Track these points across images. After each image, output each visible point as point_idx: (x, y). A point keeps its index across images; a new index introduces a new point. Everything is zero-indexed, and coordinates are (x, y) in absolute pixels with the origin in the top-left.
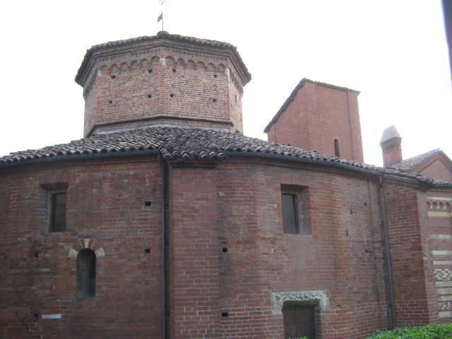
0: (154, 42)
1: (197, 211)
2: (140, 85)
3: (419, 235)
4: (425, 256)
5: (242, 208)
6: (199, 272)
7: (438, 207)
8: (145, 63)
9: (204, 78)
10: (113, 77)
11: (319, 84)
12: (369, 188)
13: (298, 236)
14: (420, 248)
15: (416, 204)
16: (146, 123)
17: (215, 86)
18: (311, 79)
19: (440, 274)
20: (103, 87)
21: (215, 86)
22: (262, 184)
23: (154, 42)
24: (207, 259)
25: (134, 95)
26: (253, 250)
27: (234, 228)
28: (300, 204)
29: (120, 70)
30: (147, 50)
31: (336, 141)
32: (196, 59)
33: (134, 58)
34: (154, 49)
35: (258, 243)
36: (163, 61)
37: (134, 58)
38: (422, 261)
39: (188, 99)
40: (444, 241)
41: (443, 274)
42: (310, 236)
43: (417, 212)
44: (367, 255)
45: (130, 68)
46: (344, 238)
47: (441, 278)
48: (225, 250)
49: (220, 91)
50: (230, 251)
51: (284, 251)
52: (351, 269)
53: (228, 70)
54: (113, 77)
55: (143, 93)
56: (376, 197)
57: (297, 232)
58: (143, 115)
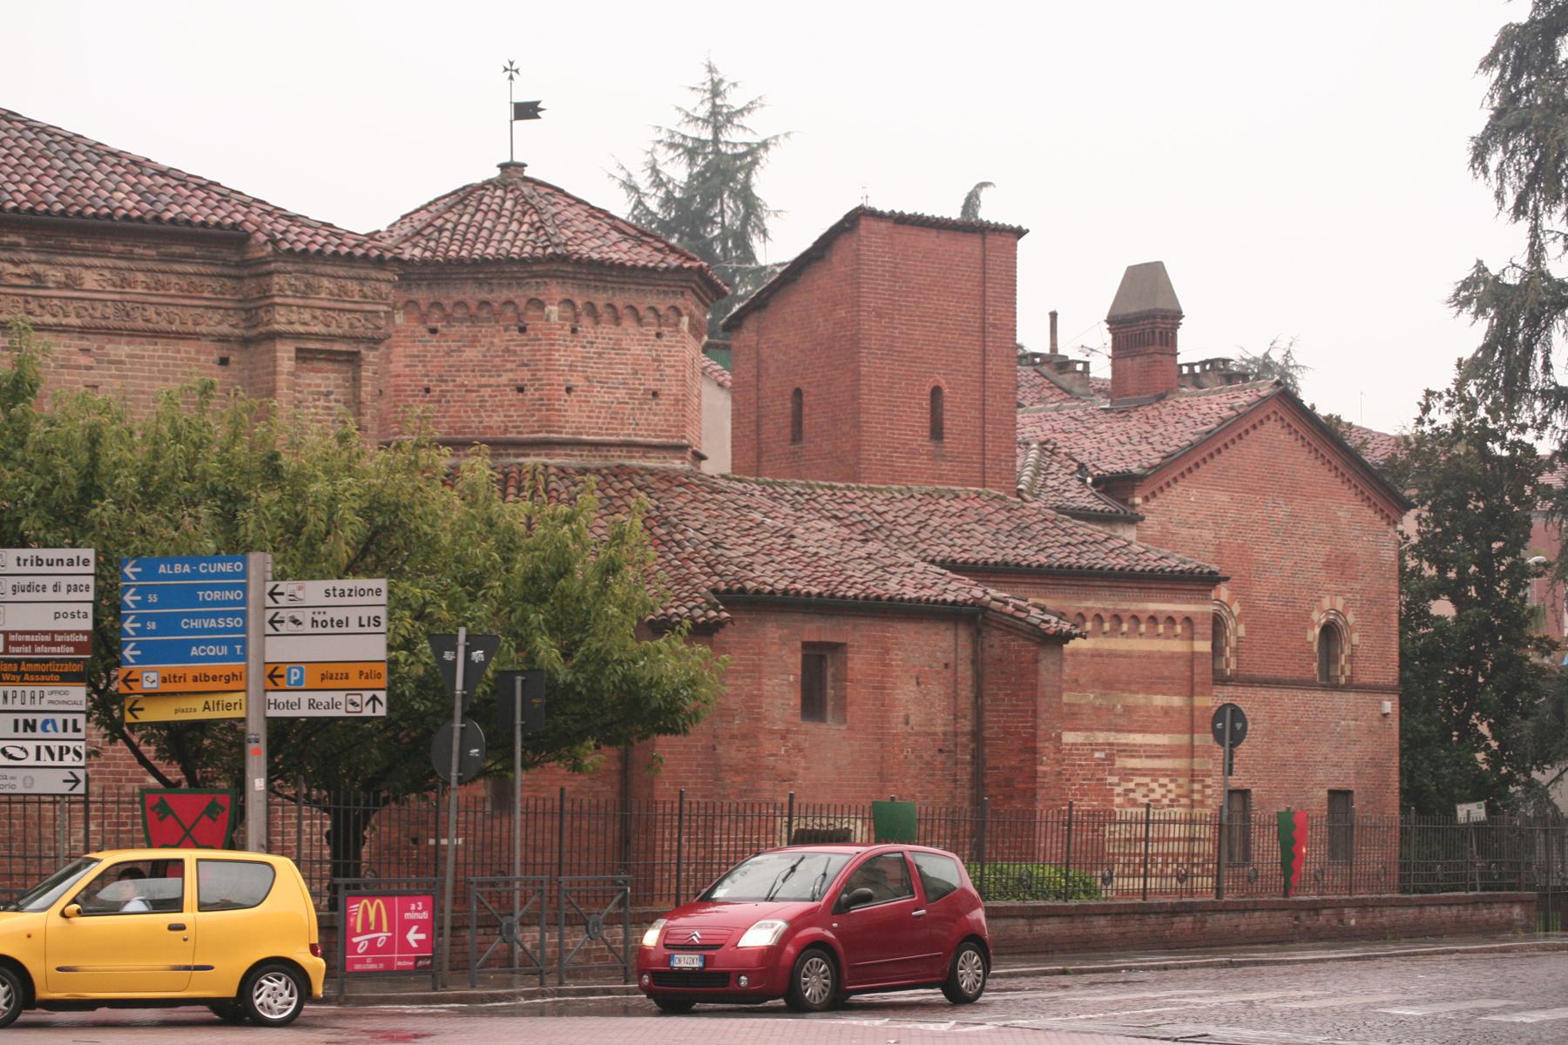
2: (498, 361)
3: (1034, 727)
5: (740, 682)
7: (1161, 628)
8: (509, 312)
9: (635, 342)
10: (434, 331)
11: (900, 220)
13: (824, 726)
14: (1034, 750)
15: (1036, 672)
18: (879, 209)
19: (1143, 790)
25: (484, 381)
28: (830, 672)
29: (448, 319)
30: (519, 281)
31: (936, 392)
33: (484, 295)
35: (761, 738)
36: (553, 310)
37: (484, 295)
38: (1036, 772)
39: (600, 396)
40: (1166, 711)
41: (1153, 791)
42: (843, 727)
43: (1034, 687)
45: (473, 319)
49: (669, 371)
50: (720, 750)
51: (801, 750)
53: (686, 319)
54: (434, 331)
55: (504, 379)
57: (823, 720)
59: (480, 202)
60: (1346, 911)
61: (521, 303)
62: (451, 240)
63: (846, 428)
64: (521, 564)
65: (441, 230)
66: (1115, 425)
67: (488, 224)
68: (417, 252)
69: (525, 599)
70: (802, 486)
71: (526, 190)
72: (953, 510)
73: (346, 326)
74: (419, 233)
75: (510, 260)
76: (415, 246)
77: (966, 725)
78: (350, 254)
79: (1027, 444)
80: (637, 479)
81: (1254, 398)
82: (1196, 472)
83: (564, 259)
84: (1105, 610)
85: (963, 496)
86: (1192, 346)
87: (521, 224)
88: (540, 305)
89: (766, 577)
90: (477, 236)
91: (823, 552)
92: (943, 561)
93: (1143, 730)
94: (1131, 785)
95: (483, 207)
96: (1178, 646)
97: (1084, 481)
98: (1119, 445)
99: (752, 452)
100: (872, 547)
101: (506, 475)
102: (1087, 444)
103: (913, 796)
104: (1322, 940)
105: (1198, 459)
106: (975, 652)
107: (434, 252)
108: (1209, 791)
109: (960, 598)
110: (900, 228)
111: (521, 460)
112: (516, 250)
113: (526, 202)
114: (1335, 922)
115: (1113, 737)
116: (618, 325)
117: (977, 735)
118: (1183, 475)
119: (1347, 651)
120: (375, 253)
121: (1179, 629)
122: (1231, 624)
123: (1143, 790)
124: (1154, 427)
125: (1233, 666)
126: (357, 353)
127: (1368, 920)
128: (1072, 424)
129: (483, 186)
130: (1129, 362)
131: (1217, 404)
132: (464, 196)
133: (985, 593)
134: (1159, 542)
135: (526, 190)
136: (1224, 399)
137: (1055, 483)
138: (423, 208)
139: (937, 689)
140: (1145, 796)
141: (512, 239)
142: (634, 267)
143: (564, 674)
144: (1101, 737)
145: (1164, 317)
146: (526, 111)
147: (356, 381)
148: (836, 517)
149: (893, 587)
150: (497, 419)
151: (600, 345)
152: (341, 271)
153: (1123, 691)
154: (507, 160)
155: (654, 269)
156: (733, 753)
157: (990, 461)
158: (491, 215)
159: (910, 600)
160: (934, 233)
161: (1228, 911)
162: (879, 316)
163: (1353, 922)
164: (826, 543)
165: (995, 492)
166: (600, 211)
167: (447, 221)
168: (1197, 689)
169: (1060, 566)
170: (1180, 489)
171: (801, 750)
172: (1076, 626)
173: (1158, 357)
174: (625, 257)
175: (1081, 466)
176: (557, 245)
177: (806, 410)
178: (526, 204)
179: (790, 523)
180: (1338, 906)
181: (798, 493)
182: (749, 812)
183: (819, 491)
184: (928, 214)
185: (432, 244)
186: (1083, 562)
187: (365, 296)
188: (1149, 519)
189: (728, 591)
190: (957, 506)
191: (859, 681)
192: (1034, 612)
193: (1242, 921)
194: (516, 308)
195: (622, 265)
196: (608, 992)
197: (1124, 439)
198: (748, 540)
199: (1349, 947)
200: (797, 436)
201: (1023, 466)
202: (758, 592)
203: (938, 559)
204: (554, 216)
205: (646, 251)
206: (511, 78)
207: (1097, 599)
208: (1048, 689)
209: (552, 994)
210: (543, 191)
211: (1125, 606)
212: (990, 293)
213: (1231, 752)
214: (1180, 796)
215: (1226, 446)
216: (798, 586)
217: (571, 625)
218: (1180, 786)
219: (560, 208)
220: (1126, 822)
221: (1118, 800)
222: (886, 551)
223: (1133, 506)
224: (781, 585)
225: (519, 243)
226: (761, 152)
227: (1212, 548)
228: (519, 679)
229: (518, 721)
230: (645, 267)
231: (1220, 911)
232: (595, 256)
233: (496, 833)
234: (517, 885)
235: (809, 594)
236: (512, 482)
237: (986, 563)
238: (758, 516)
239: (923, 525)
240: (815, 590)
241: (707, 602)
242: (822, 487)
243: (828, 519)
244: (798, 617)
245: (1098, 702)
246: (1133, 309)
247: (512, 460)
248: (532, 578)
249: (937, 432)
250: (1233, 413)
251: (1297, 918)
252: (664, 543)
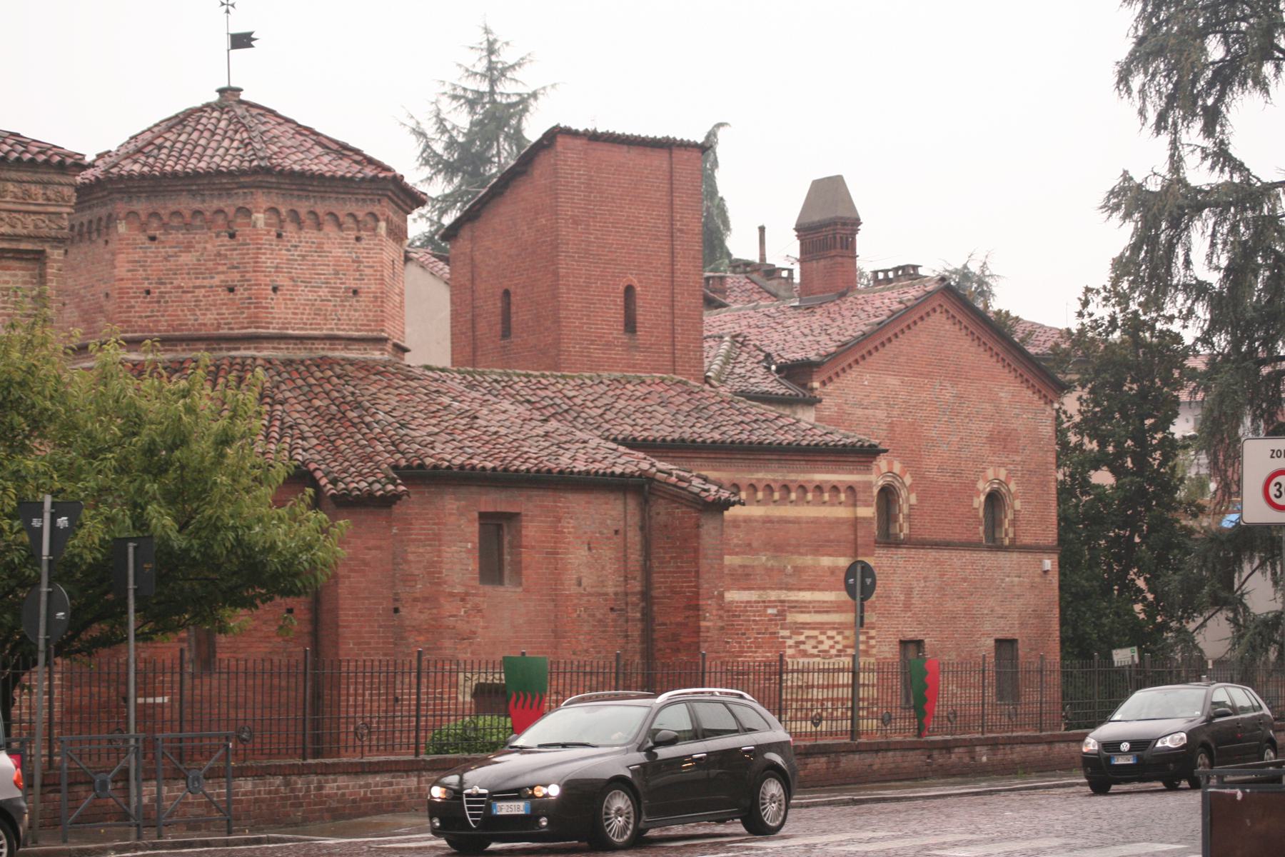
0: (242, 180)
1: (367, 564)
2: (210, 264)
4: (705, 619)
6: (369, 643)
7: (826, 496)
8: (220, 220)
9: (336, 246)
10: (153, 239)
11: (594, 137)
12: (625, 504)
13: (501, 589)
14: (697, 608)
15: (698, 536)
16: (224, 346)
17: (357, 261)
18: (574, 128)
19: (813, 642)
20: (131, 257)
21: (357, 261)
22: (451, 514)
23: (242, 180)
24: (380, 626)
25: (198, 282)
26: (435, 611)
27: (409, 579)
28: (507, 539)
30: (226, 192)
31: (629, 290)
32: (321, 209)
33: (197, 205)
34: (241, 191)
35: (442, 600)
36: (260, 218)
38: (699, 627)
39: (304, 294)
40: (833, 571)
41: (821, 642)
42: (520, 589)
43: (696, 550)
44: (612, 615)
45: (188, 227)
46: (574, 589)
47: (815, 651)
48: (396, 610)
49: (368, 271)
50: (403, 612)
51: (479, 611)
52: (581, 637)
53: (383, 225)
54: (153, 239)
55: (217, 280)
56: (637, 519)
57: (501, 583)
58: (219, 327)
59: (198, 122)
60: (978, 749)
61: (230, 211)
62: (169, 156)
63: (548, 323)
64: (140, 441)
65: (160, 147)
66: (801, 320)
67: (203, 142)
68: (137, 167)
69: (146, 470)
70: (500, 375)
71: (240, 111)
72: (638, 394)
73: (31, 227)
74: (139, 151)
75: (219, 173)
76: (135, 162)
77: (636, 586)
78: (32, 161)
79: (721, 337)
80: (338, 370)
81: (921, 293)
82: (869, 359)
83: (268, 171)
84: (774, 481)
85: (649, 382)
86: (874, 252)
87: (232, 140)
88: (248, 213)
89: (446, 454)
90: (192, 153)
91: (503, 431)
92: (624, 439)
93: (812, 588)
94: (802, 638)
95: (200, 127)
96: (842, 512)
97: (768, 368)
98: (801, 337)
99: (469, 345)
100: (553, 424)
101: (218, 367)
102: (776, 336)
103: (587, 651)
104: (954, 776)
105: (870, 347)
106: (643, 519)
107: (152, 167)
108: (873, 642)
109: (628, 471)
110: (594, 145)
111: (233, 353)
112: (225, 164)
113: (239, 122)
114: (967, 759)
115: (784, 595)
116: (320, 230)
117: (646, 595)
118: (857, 362)
119: (1010, 516)
120: (57, 158)
121: (843, 497)
122: (903, 493)
123: (813, 642)
124: (833, 320)
125: (906, 531)
126: (43, 252)
127: (999, 757)
128: (766, 321)
129: (201, 109)
130: (815, 264)
131: (890, 300)
132: (181, 120)
133: (652, 465)
134: (837, 421)
135: (240, 111)
136: (895, 295)
137: (743, 371)
138: (150, 130)
139: (607, 553)
140: (815, 647)
141: (224, 155)
142: (333, 178)
143: (179, 542)
144: (773, 595)
145: (844, 224)
146: (241, 41)
147: (42, 279)
148: (528, 401)
149: (565, 461)
150: (210, 318)
151: (303, 248)
152: (25, 176)
153: (792, 553)
154: (225, 85)
155: (352, 179)
156: (416, 614)
157: (681, 354)
158: (207, 134)
159: (579, 472)
160: (625, 148)
161: (861, 752)
162: (576, 223)
163: (984, 759)
164: (508, 424)
165: (679, 378)
166: (306, 128)
167: (166, 139)
168: (860, 551)
169: (733, 442)
170: (854, 374)
171: (479, 611)
172: (735, 494)
173: (840, 259)
174: (325, 169)
175: (768, 356)
176: (262, 159)
177: (513, 309)
178: (238, 123)
179: (476, 406)
180: (970, 745)
181: (496, 381)
182: (432, 669)
183: (516, 379)
184: (619, 131)
185: (151, 160)
186: (754, 438)
187: (48, 199)
188: (827, 401)
189: (409, 467)
190: (644, 389)
191: (533, 547)
192: (696, 482)
193: (876, 761)
194: (226, 216)
195: (322, 176)
196: (207, 844)
197: (807, 331)
198: (434, 421)
199: (975, 782)
200: (506, 332)
201: (715, 356)
202: (435, 467)
203: (620, 437)
204: (263, 133)
205: (345, 163)
206: (228, 12)
207: (767, 471)
208: (710, 552)
209: (146, 848)
210: (255, 111)
211: (793, 476)
212: (677, 201)
213: (862, 606)
214: (846, 647)
215: (896, 336)
216: (475, 461)
217: (188, 492)
218: (846, 638)
219: (270, 126)
220: (798, 671)
221: (790, 652)
222: (563, 430)
223: (812, 389)
224: (457, 462)
225: (228, 158)
226: (532, 101)
227: (885, 427)
228: (131, 546)
229: (131, 586)
230: (343, 177)
231: (853, 752)
232: (297, 168)
233: (197, 692)
234: (132, 742)
235: (484, 468)
236: (222, 374)
237: (664, 440)
238: (446, 400)
239: (609, 407)
240: (489, 465)
241: (386, 477)
242: (519, 376)
243: (521, 403)
244: (474, 489)
245: (769, 564)
246: (816, 218)
247: (225, 353)
248: (150, 450)
249: (630, 325)
250: (902, 306)
251: (929, 757)
252: (354, 425)
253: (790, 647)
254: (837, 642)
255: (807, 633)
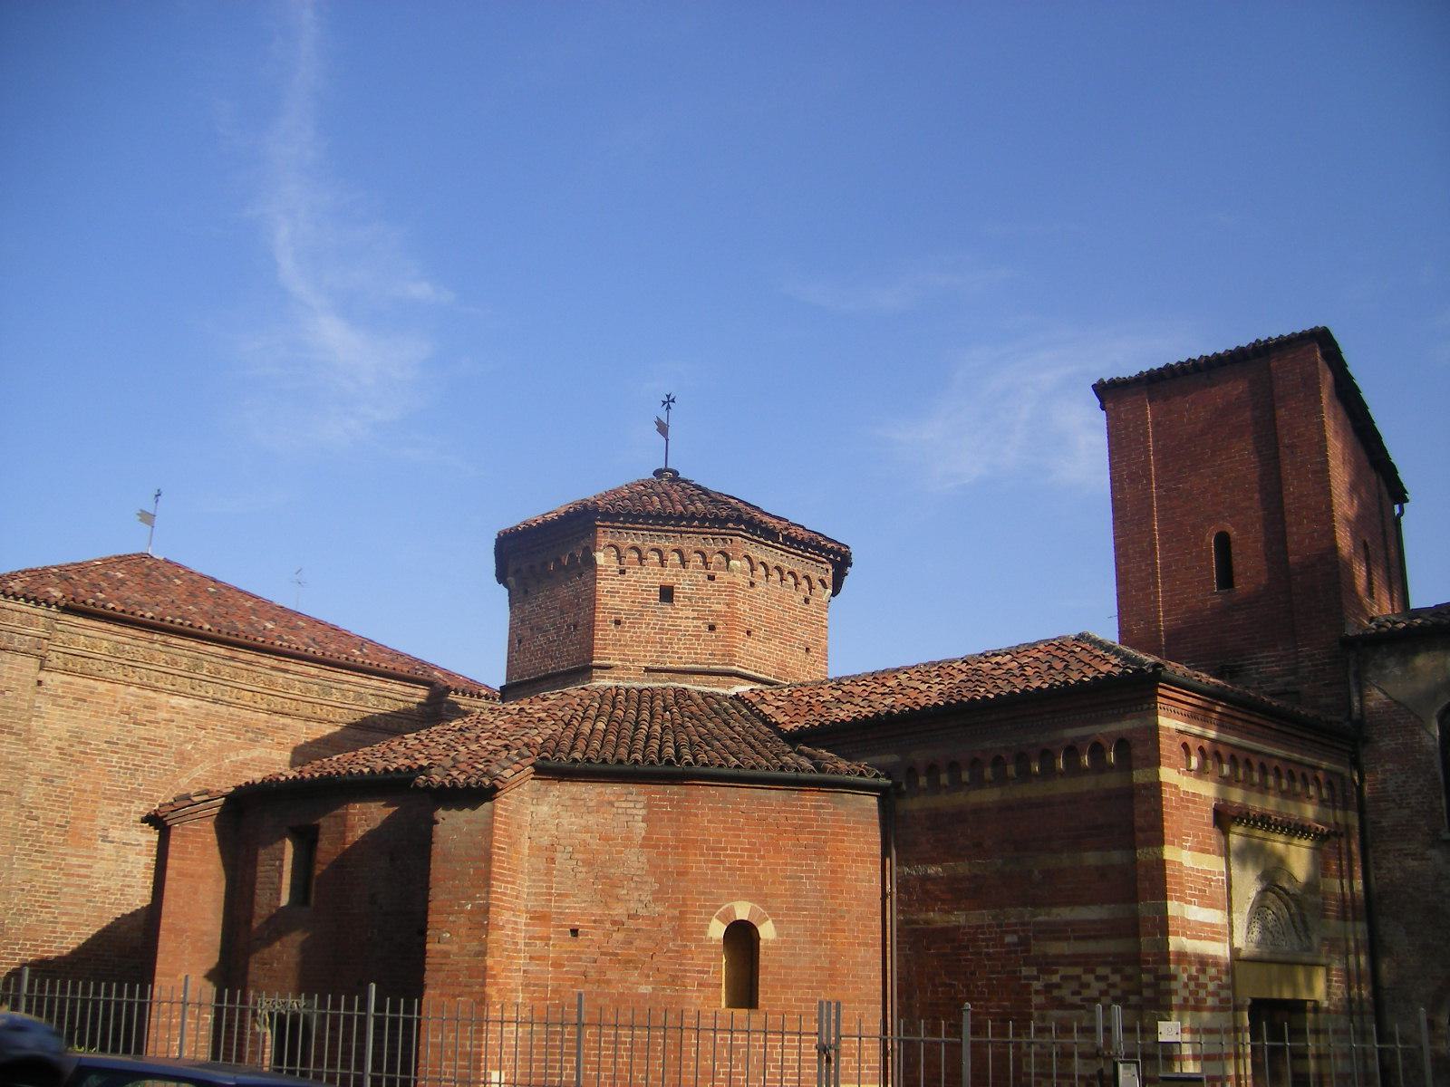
19: (1074, 985)
41: (1087, 986)
47: (1076, 999)
93: (1073, 901)
94: (1056, 979)
123: (1074, 985)
140: (1074, 993)
154: (663, 467)
218: (1126, 978)
221: (1037, 1000)
253: (1037, 992)
254: (1113, 986)
255: (1063, 971)
